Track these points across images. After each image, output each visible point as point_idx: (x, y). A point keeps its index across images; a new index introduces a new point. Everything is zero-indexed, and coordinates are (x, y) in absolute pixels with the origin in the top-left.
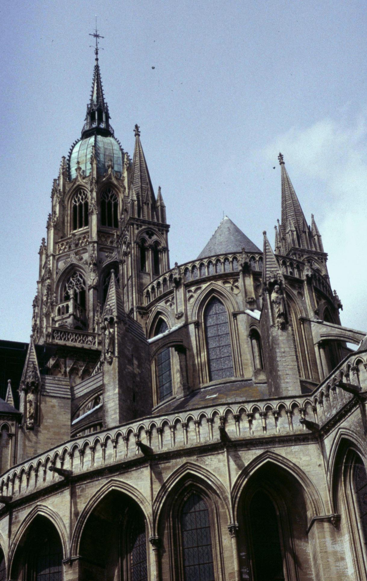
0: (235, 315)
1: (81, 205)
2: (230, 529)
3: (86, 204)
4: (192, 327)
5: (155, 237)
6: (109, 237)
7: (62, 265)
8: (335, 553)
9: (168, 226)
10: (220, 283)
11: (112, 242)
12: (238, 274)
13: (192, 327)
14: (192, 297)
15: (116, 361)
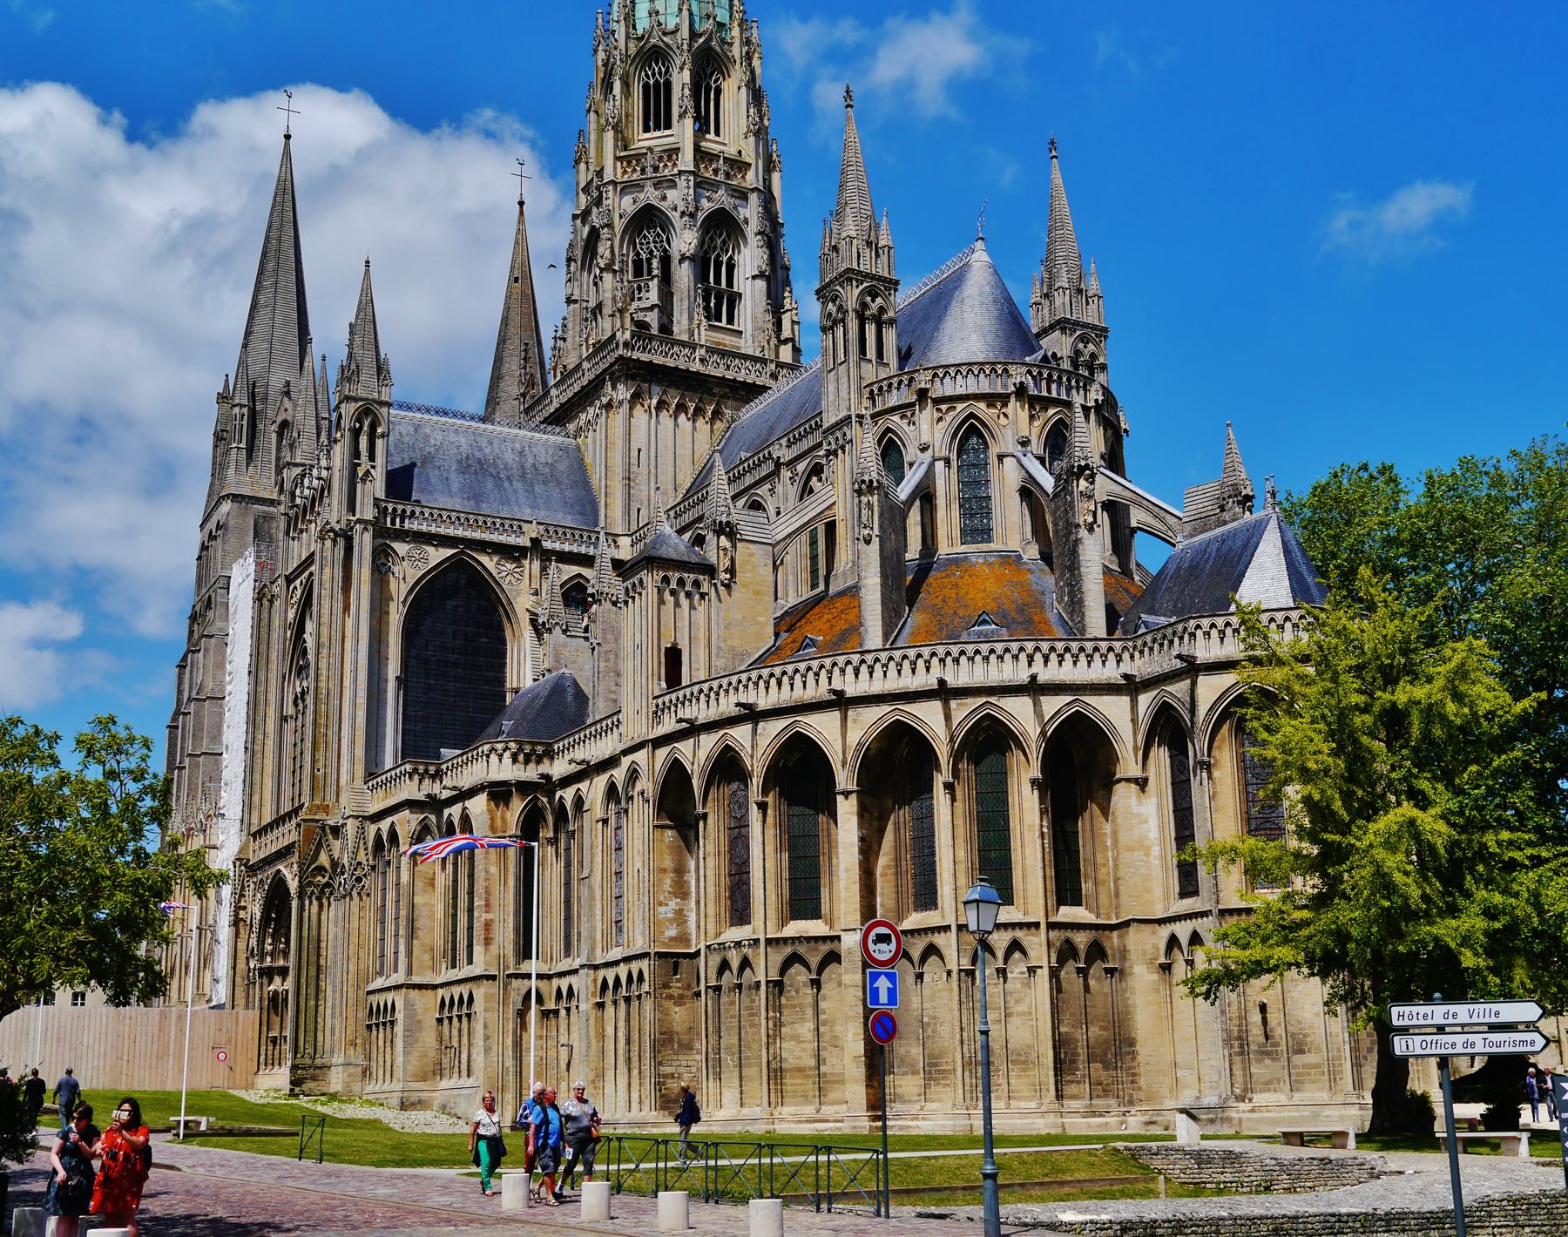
0: (1001, 457)
1: (657, 83)
2: (1034, 782)
3: (668, 85)
4: (940, 465)
5: (879, 300)
6: (711, 161)
7: (628, 205)
8: (1139, 815)
9: (897, 283)
10: (982, 405)
11: (716, 171)
12: (1008, 396)
13: (940, 465)
14: (940, 419)
15: (876, 541)
